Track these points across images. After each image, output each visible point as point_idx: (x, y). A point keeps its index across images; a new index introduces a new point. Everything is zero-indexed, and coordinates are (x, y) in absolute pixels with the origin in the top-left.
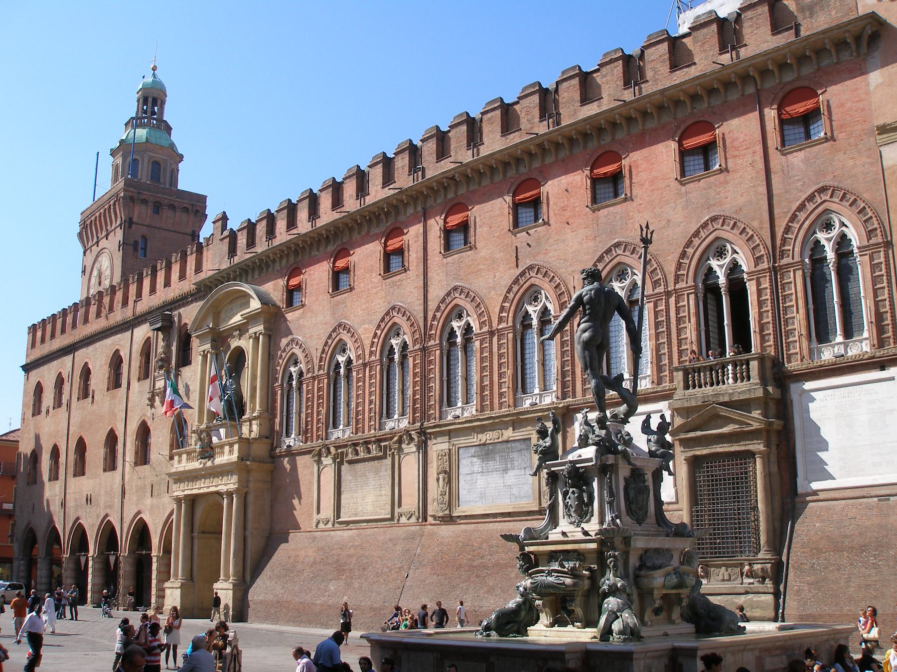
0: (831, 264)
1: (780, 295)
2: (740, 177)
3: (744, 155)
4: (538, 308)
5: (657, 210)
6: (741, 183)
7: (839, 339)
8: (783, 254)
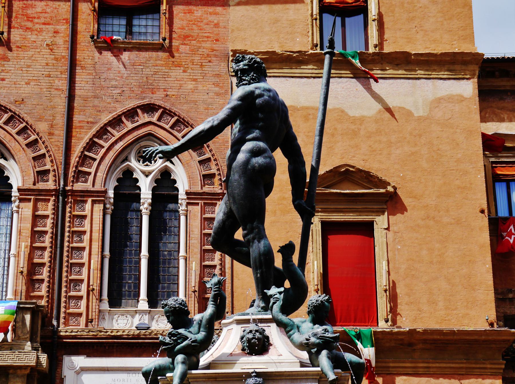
0: (146, 205)
1: (67, 229)
2: (29, 58)
3: (41, 31)
6: (29, 66)
7: (143, 305)
8: (80, 175)
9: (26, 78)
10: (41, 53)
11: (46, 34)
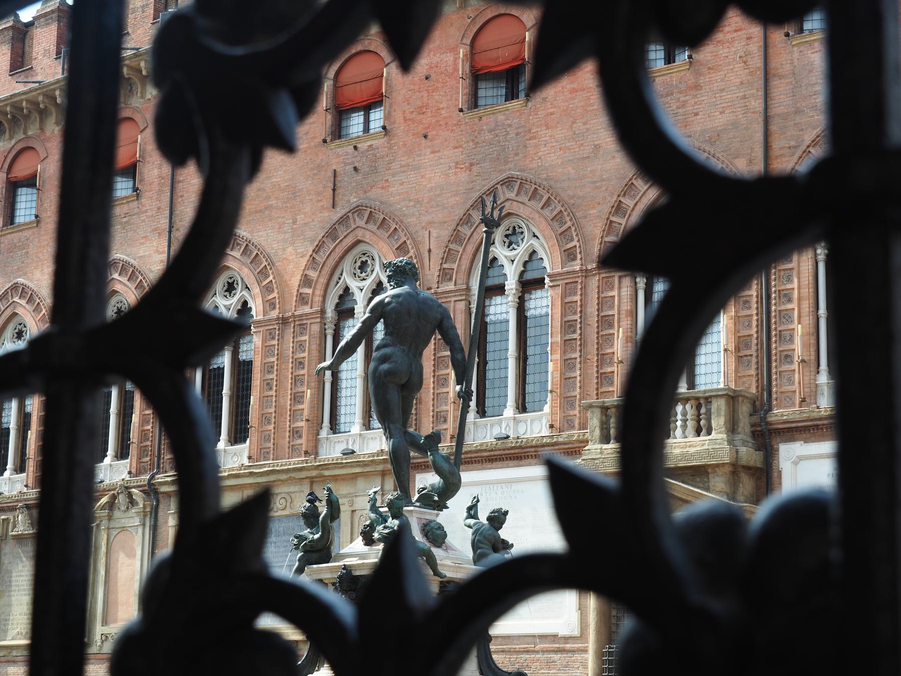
4: (367, 283)
5: (579, 126)
6: (722, 90)
9: (721, 106)
10: (735, 70)
11: (739, 43)
